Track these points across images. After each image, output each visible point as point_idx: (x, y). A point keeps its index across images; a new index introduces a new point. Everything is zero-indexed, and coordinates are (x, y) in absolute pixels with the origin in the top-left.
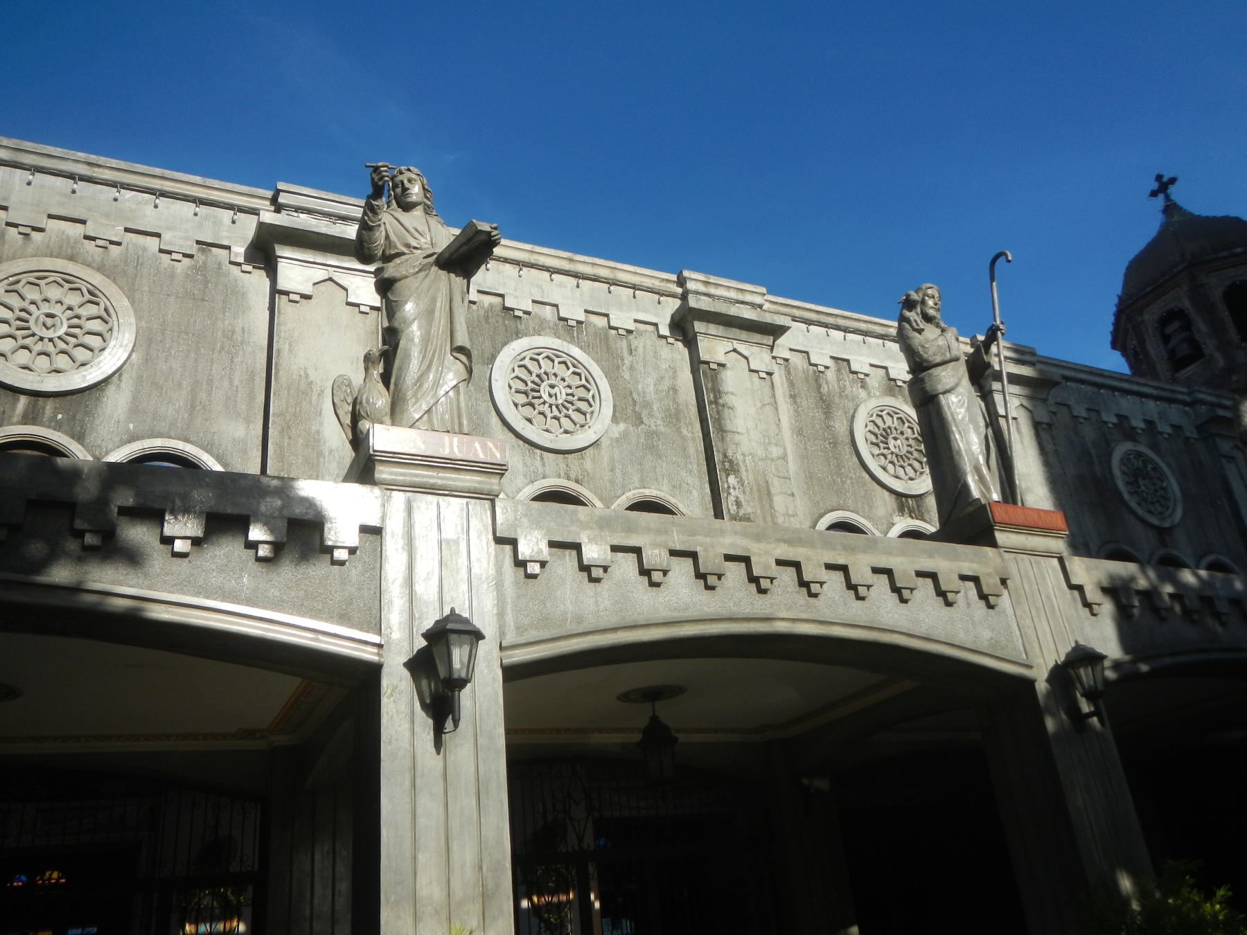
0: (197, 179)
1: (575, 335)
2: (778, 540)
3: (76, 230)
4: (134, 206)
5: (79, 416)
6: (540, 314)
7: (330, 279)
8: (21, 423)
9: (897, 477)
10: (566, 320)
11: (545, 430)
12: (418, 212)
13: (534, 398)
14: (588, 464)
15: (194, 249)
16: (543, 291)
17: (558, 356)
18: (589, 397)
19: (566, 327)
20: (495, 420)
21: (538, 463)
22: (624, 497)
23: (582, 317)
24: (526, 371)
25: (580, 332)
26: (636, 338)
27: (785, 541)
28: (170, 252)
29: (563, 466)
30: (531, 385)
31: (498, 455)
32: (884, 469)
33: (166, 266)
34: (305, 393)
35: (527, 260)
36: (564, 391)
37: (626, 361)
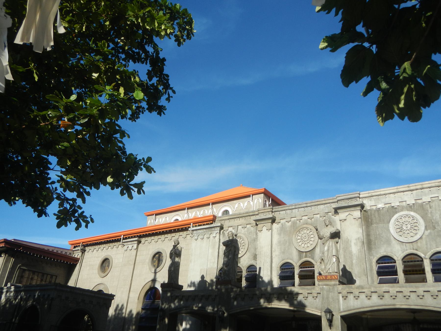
0: (323, 199)
1: (413, 208)
2: (397, 287)
3: (306, 218)
4: (314, 209)
5: (312, 255)
6: (402, 205)
7: (349, 214)
8: (305, 258)
10: (409, 204)
11: (405, 238)
12: (329, 226)
13: (402, 229)
14: (419, 244)
16: (402, 198)
17: (407, 216)
18: (417, 225)
19: (410, 207)
20: (392, 238)
21: (404, 247)
22: (430, 252)
23: (414, 202)
24: (399, 222)
25: (414, 206)
26: (432, 203)
27: (399, 287)
28: (321, 217)
29: (411, 246)
30: (401, 226)
31: (337, 278)
33: (321, 220)
34: (348, 242)
35: (396, 191)
36: (410, 225)
37: (429, 211)
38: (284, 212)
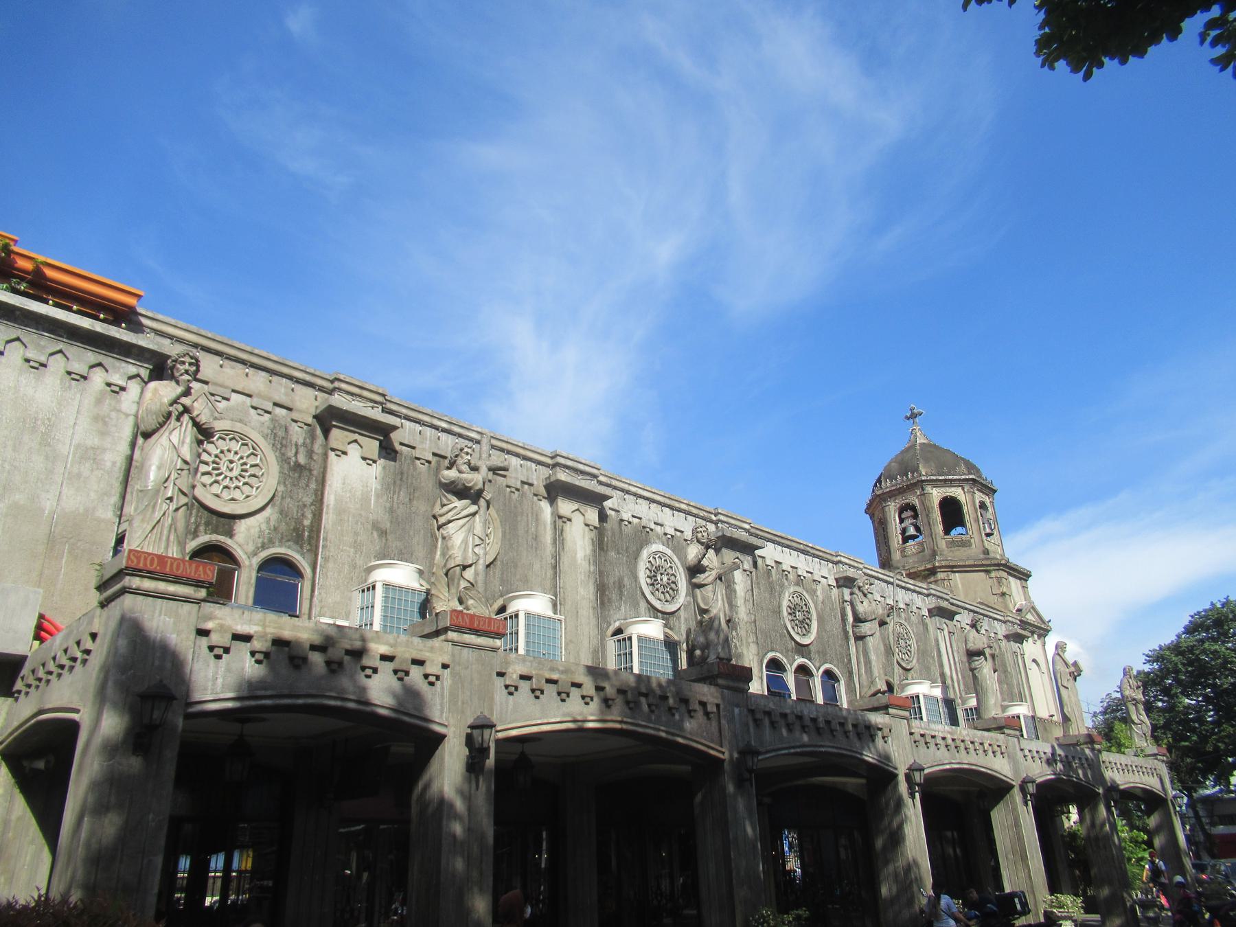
9: (798, 633)
15: (519, 485)
32: (793, 628)
38: (418, 427)
